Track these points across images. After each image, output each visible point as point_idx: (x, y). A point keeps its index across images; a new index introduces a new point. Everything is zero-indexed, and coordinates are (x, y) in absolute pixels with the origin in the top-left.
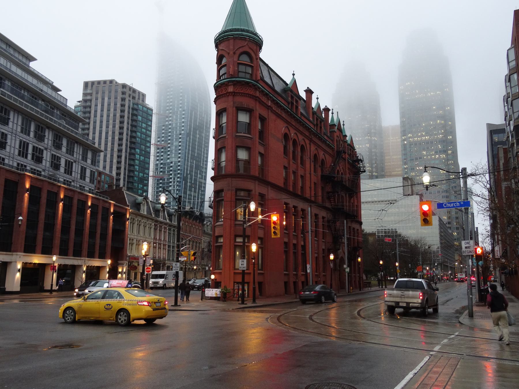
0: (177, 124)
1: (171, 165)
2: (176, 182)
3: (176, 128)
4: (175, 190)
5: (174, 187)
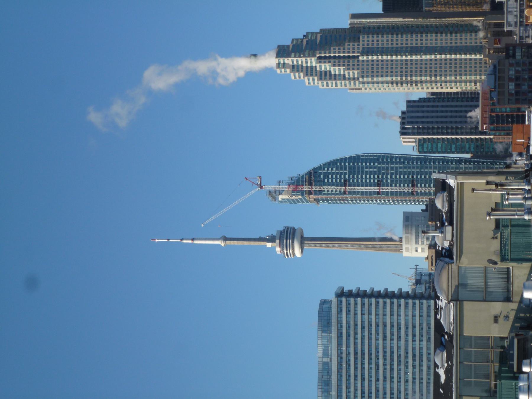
0: (392, 169)
3: (397, 168)
4: (465, 166)
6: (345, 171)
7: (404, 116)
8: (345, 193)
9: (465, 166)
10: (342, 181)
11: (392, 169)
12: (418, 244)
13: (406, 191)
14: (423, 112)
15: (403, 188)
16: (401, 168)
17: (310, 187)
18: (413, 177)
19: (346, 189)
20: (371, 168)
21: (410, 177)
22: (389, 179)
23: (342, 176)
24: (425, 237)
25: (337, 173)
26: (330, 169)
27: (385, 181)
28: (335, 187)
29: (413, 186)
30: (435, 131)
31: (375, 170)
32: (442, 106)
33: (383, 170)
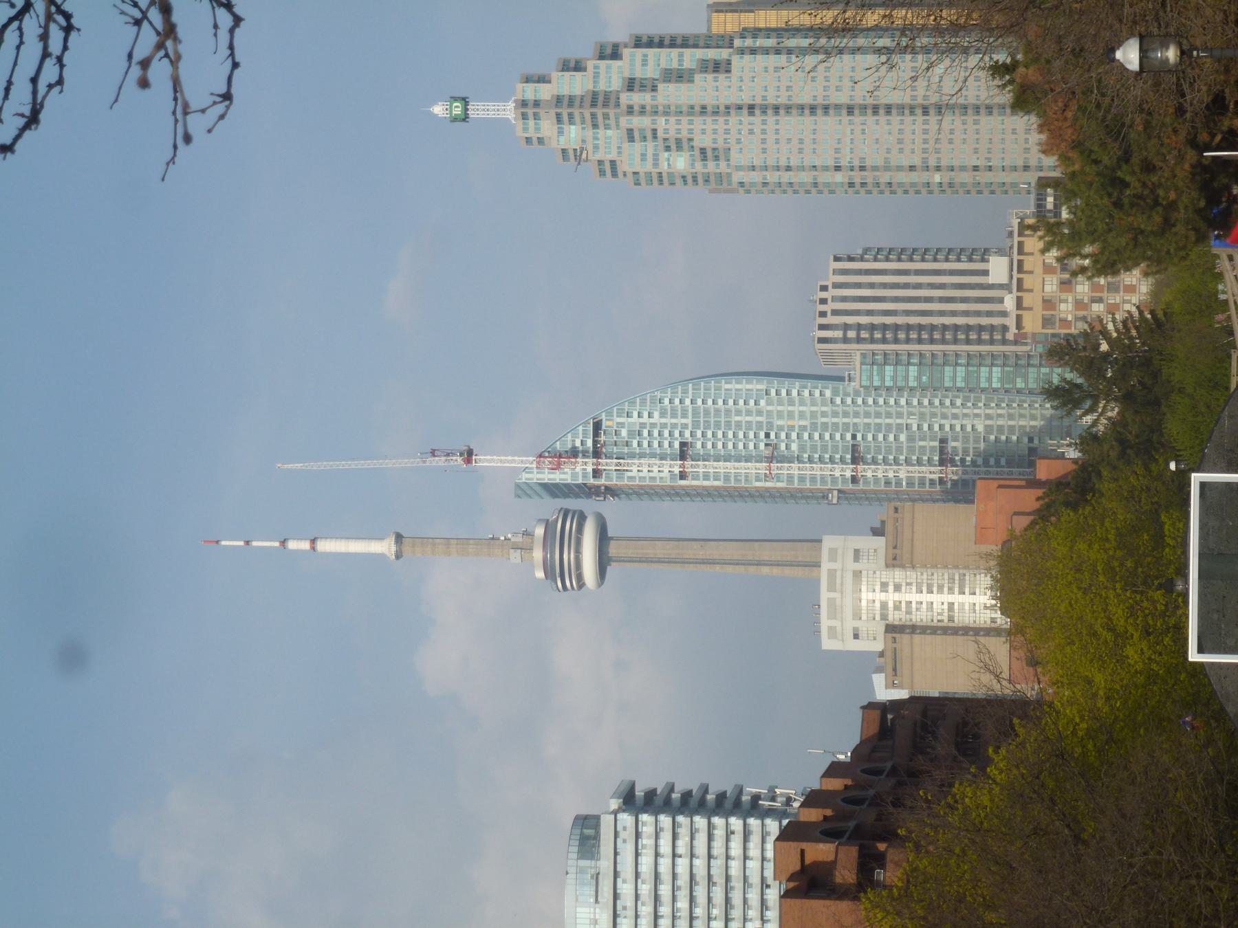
0: (802, 415)
1: (915, 428)
2: (965, 411)
4: (988, 411)
5: (977, 415)
6: (684, 421)
7: (823, 295)
8: (683, 476)
9: (988, 411)
10: (677, 445)
11: (802, 415)
12: (860, 618)
13: (837, 474)
14: (872, 286)
15: (829, 466)
16: (824, 414)
17: (595, 460)
18: (854, 437)
19: (683, 466)
20: (749, 413)
21: (849, 437)
22: (794, 441)
23: (677, 434)
24: (878, 605)
25: (664, 426)
26: (646, 414)
27: (783, 447)
28: (658, 462)
29: (855, 460)
30: (902, 336)
31: (759, 419)
32: (918, 272)
33: (778, 419)
